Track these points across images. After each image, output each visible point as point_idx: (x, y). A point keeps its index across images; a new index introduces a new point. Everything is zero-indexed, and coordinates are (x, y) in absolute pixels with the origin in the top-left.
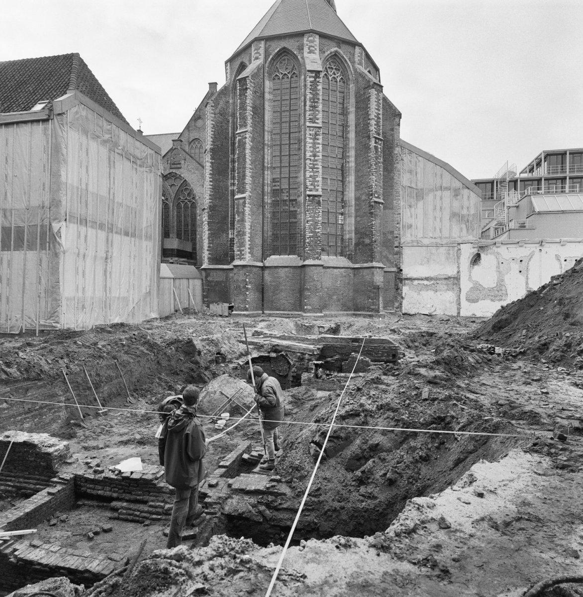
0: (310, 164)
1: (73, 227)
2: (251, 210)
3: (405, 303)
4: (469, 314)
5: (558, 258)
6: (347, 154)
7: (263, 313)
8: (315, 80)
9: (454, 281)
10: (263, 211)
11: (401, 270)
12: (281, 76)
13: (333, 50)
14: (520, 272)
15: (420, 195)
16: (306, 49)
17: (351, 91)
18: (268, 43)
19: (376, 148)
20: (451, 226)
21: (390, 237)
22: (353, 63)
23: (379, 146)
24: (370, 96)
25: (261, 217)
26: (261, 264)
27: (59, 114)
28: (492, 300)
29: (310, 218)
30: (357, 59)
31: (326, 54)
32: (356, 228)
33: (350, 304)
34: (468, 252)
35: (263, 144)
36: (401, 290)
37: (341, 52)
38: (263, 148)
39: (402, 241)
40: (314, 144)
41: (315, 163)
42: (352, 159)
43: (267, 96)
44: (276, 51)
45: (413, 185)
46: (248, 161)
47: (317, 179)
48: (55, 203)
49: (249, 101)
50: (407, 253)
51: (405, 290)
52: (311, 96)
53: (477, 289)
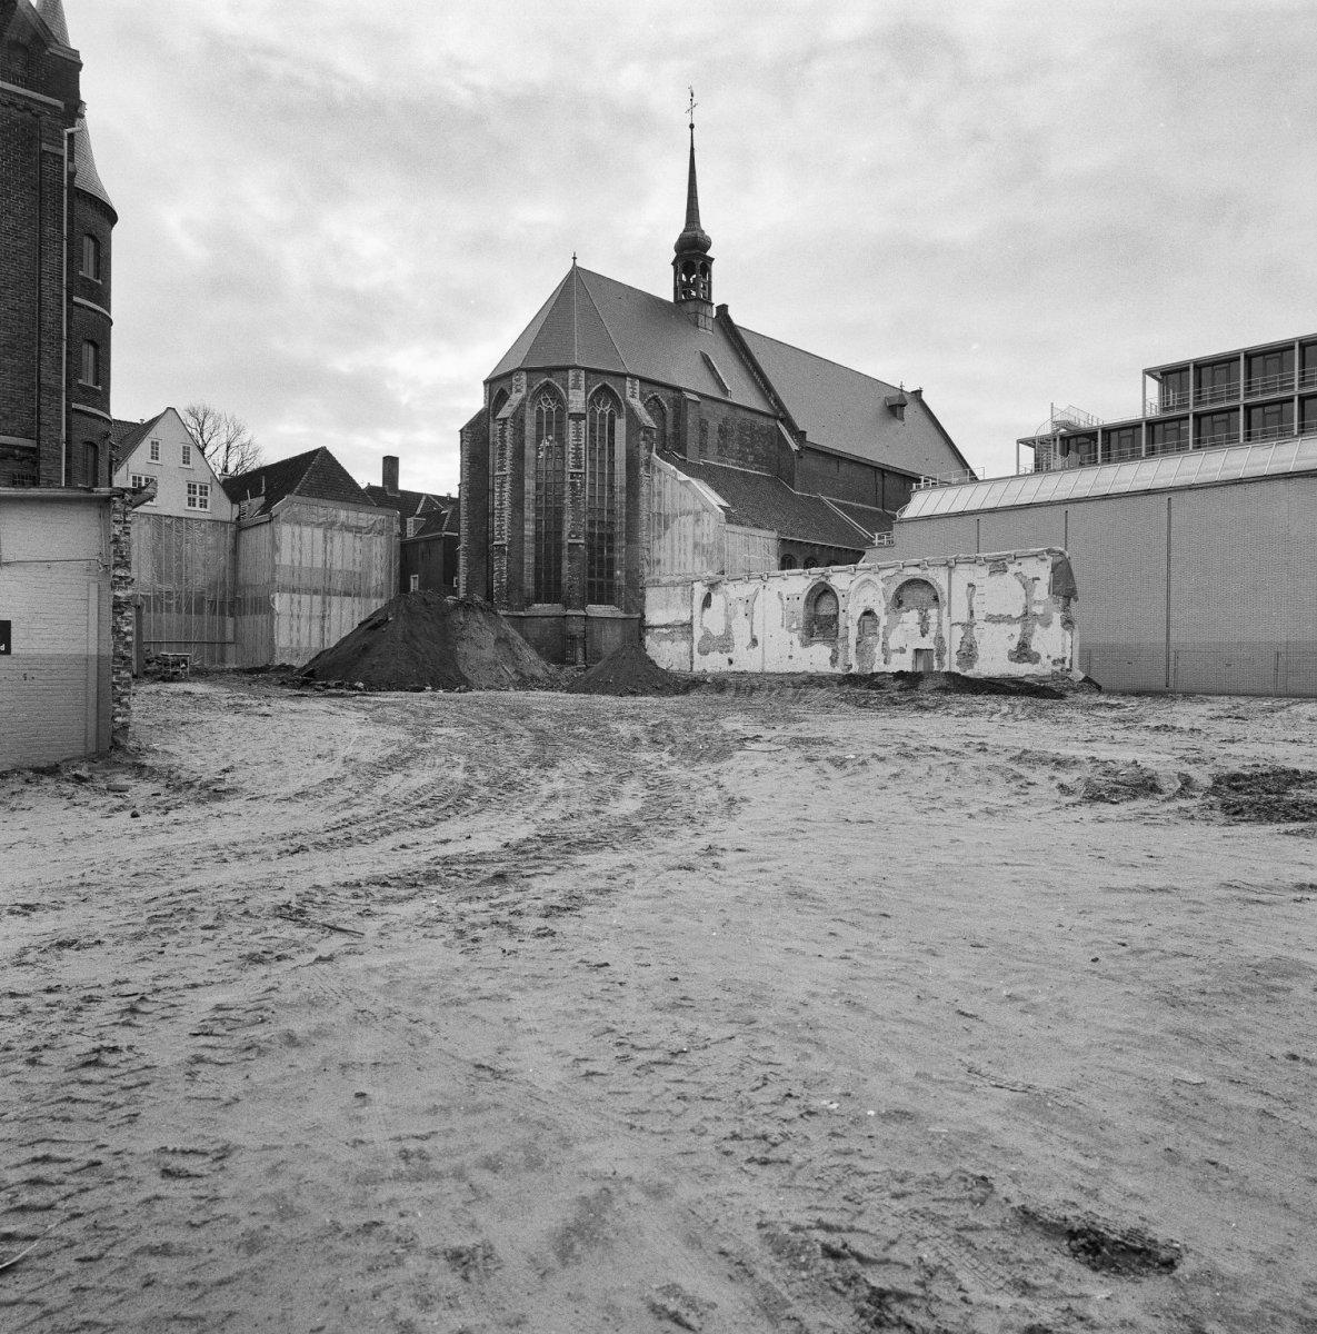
1: (286, 596)
9: (687, 627)
19: (573, 485)
22: (566, 389)
34: (700, 590)
40: (501, 492)
50: (652, 595)
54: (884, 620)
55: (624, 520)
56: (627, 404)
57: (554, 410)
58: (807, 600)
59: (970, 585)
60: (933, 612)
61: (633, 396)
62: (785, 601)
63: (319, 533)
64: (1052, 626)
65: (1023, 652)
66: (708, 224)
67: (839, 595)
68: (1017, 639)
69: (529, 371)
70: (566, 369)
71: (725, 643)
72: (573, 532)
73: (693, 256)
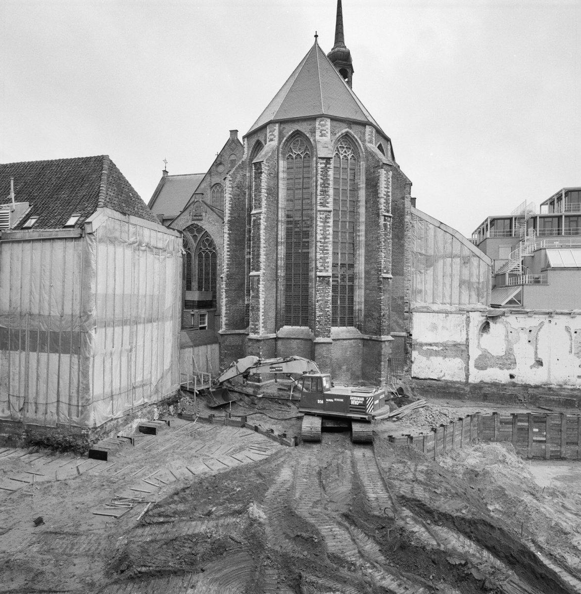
0: (321, 246)
1: (101, 331)
2: (265, 286)
4: (477, 381)
5: (567, 329)
6: (358, 228)
7: (276, 382)
8: (326, 166)
10: (277, 285)
11: (411, 335)
12: (294, 156)
13: (344, 131)
14: (529, 341)
15: (429, 262)
16: (318, 133)
17: (361, 167)
18: (282, 126)
19: (385, 225)
20: (460, 292)
21: (400, 302)
22: (364, 141)
23: (388, 223)
24: (379, 176)
25: (275, 290)
26: (273, 336)
27: (90, 234)
28: (501, 368)
29: (320, 298)
30: (367, 137)
31: (338, 135)
32: (365, 301)
33: (359, 373)
34: (477, 319)
35: (277, 221)
37: (352, 133)
38: (277, 224)
39: (412, 307)
40: (324, 227)
41: (325, 245)
42: (363, 233)
43: (281, 175)
44: (290, 133)
45: (423, 252)
46: (262, 241)
47: (327, 260)
48: (85, 314)
49: (264, 185)
51: (415, 354)
52: (322, 181)
53: (486, 357)
63: (129, 252)
69: (282, 122)
71: (507, 361)
72: (385, 268)
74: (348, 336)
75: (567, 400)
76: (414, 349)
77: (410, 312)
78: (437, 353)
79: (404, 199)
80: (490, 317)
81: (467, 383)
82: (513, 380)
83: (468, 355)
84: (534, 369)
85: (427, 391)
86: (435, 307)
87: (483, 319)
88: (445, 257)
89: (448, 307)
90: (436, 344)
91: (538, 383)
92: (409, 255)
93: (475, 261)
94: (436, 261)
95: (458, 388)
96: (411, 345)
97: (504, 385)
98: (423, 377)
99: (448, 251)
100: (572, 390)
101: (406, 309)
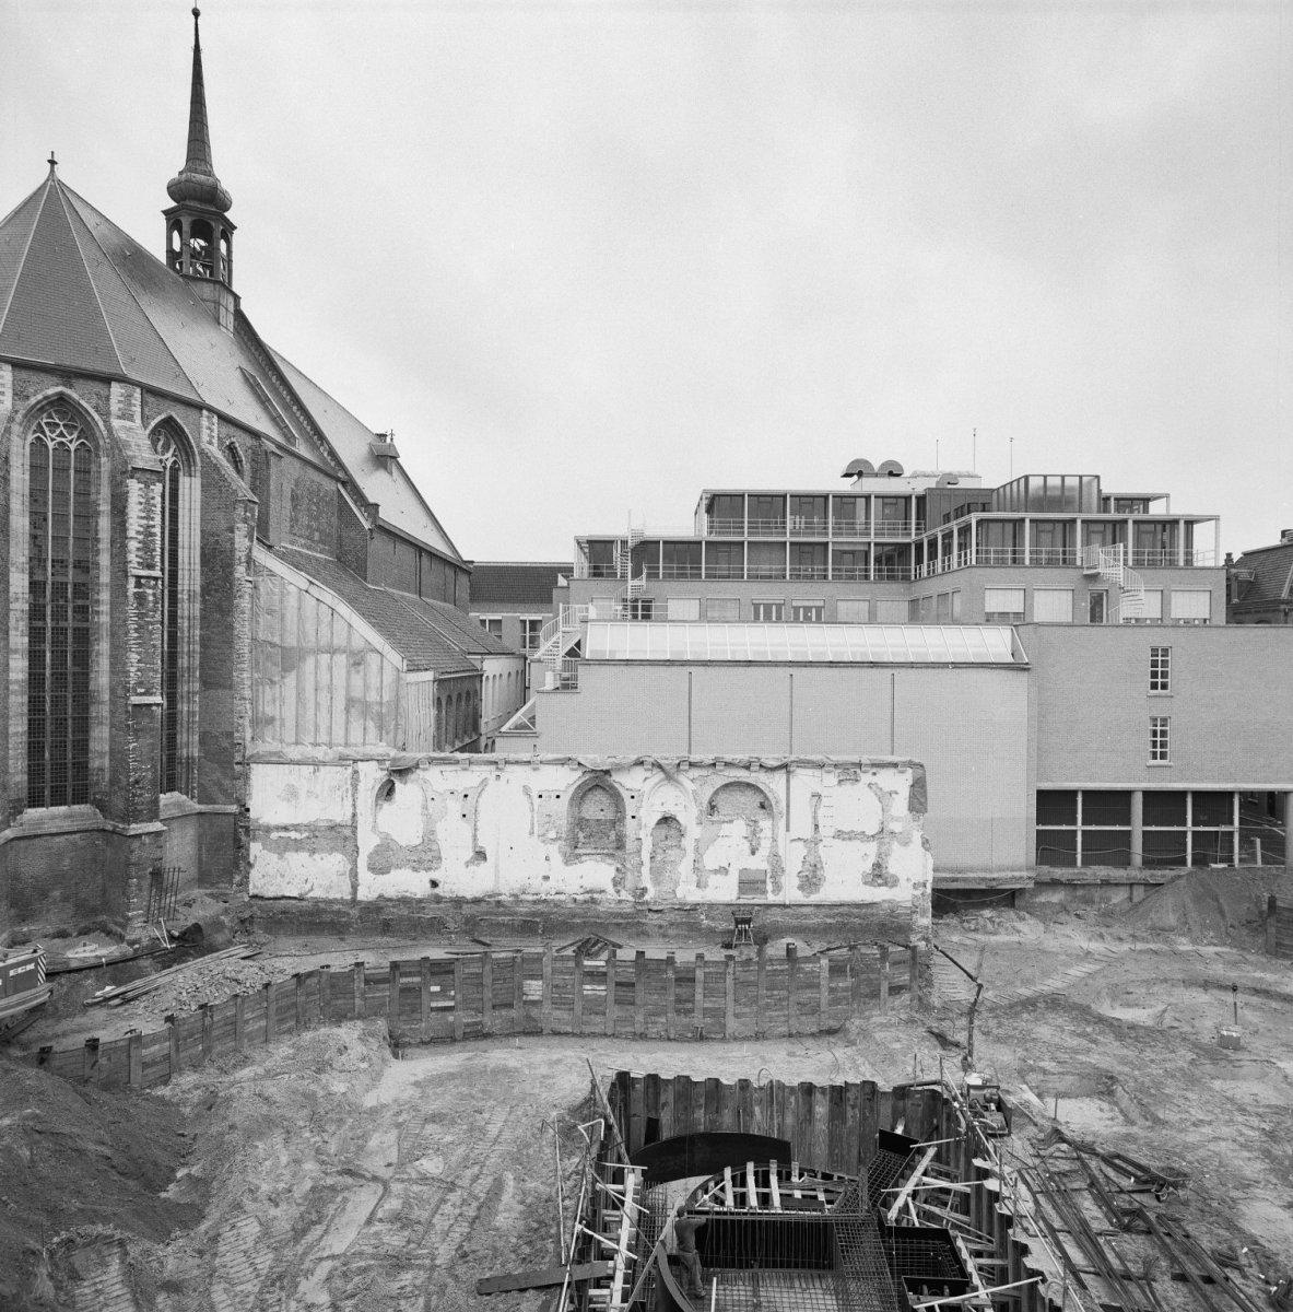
3: (254, 874)
5: (527, 791)
6: (96, 597)
11: (248, 810)
14: (464, 816)
17: (103, 469)
19: (140, 598)
20: (347, 722)
21: (225, 744)
22: (106, 415)
23: (150, 591)
24: (128, 492)
28: (415, 870)
30: (115, 407)
31: (33, 401)
34: (372, 775)
36: (248, 850)
37: (75, 396)
39: (248, 753)
42: (105, 608)
45: (276, 640)
51: (255, 848)
53: (388, 848)
54: (693, 831)
55: (197, 648)
56: (202, 452)
57: (72, 447)
58: (572, 799)
59: (817, 796)
60: (765, 824)
61: (210, 443)
62: (537, 801)
64: (912, 846)
65: (878, 875)
66: (227, 169)
67: (626, 795)
68: (872, 860)
70: (107, 380)
71: (425, 855)
72: (140, 684)
73: (200, 210)
74: (66, 826)
75: (525, 921)
76: (254, 839)
77: (246, 763)
78: (297, 846)
79: (233, 532)
80: (394, 771)
81: (354, 902)
82: (437, 891)
83: (356, 846)
84: (472, 868)
85: (280, 922)
86: (293, 753)
87: (382, 776)
88: (318, 651)
89: (320, 753)
90: (296, 828)
91: (479, 895)
92: (244, 646)
93: (373, 659)
94: (302, 659)
95: (338, 912)
96: (247, 830)
97: (420, 901)
98: (271, 895)
99: (324, 642)
100: (535, 902)
101: (238, 758)
